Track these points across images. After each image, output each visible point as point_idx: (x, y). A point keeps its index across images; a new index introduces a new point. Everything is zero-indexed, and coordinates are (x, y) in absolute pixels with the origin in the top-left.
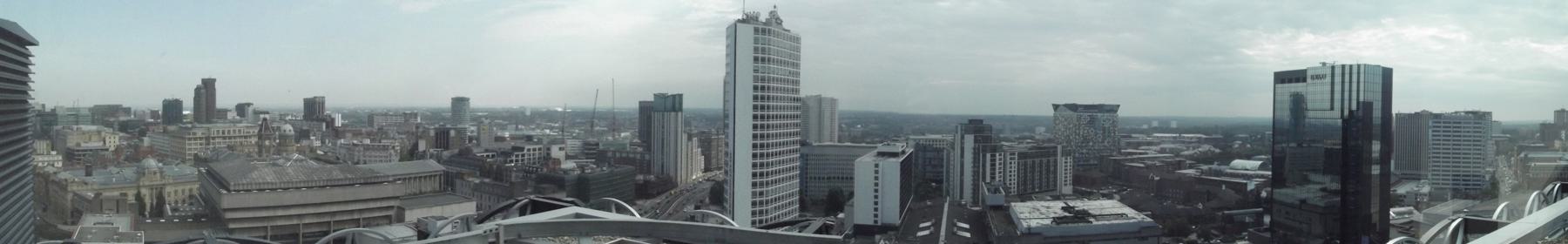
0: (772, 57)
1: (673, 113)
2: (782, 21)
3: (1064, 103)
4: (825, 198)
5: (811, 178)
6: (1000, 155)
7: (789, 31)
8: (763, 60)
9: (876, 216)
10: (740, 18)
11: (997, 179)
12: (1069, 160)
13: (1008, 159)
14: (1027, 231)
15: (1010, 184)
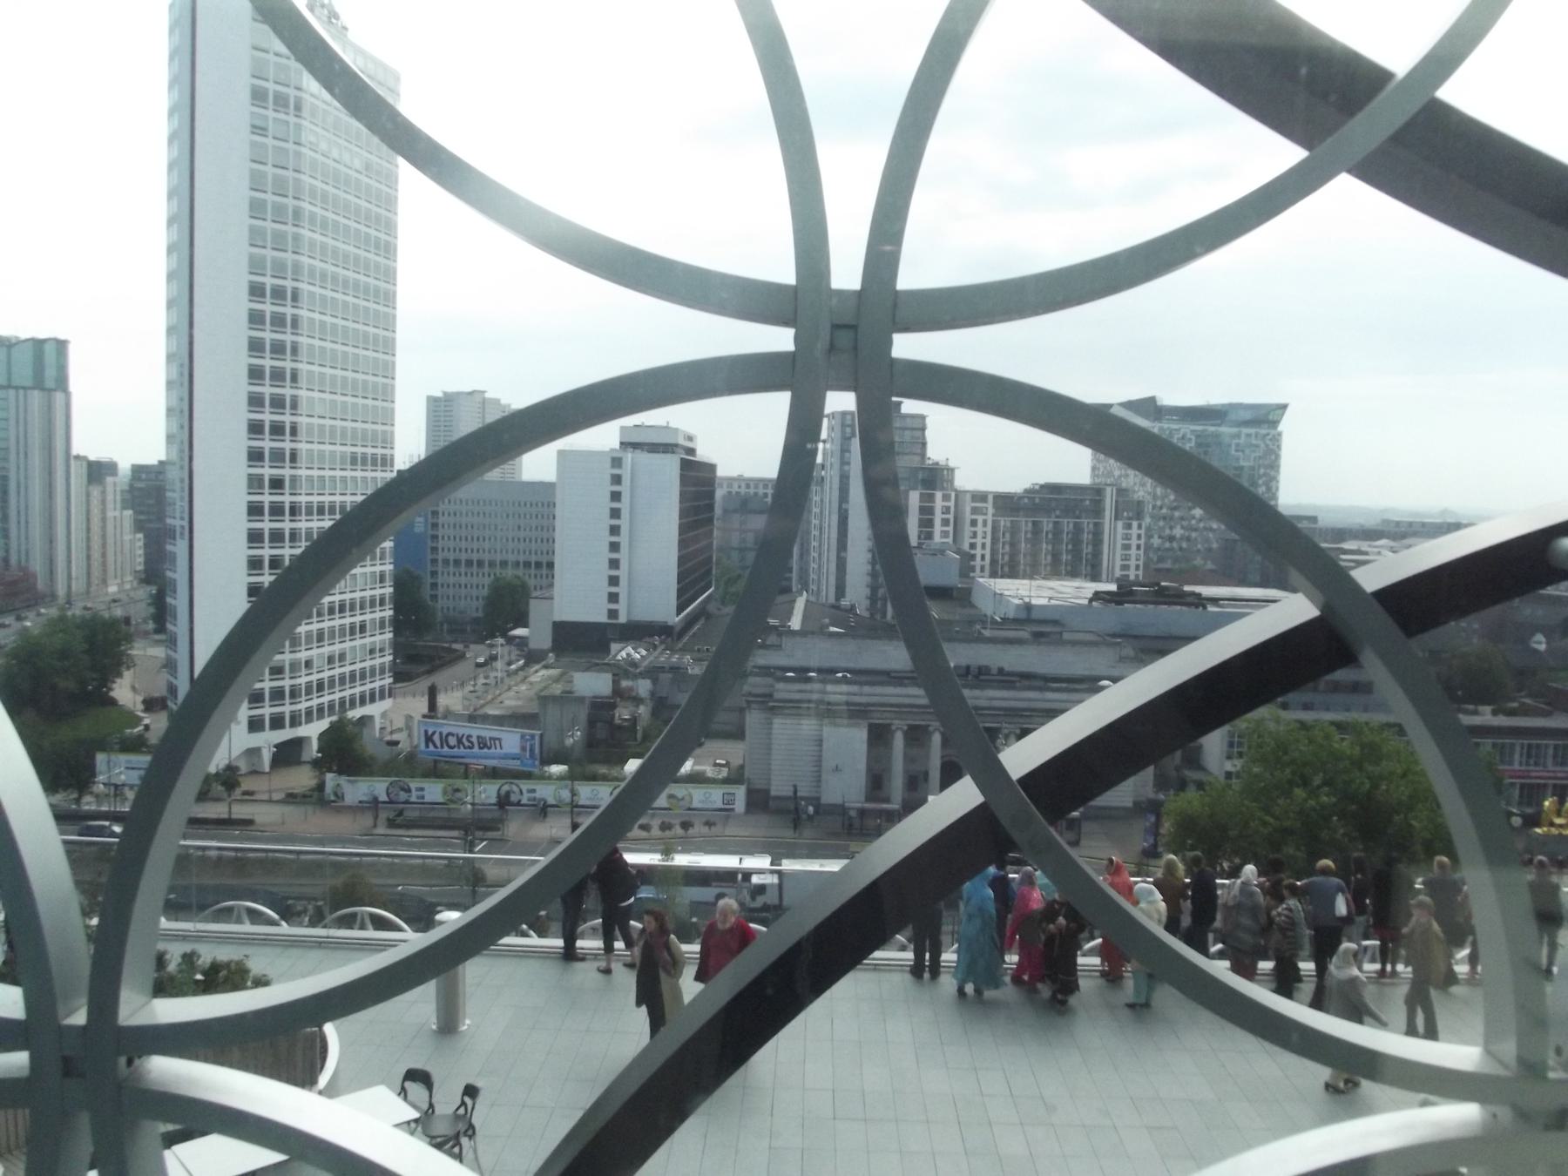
1: (36, 397)
4: (480, 614)
5: (446, 562)
6: (946, 498)
9: (613, 598)
11: (937, 538)
12: (1134, 531)
13: (968, 509)
14: (1023, 615)
15: (973, 546)
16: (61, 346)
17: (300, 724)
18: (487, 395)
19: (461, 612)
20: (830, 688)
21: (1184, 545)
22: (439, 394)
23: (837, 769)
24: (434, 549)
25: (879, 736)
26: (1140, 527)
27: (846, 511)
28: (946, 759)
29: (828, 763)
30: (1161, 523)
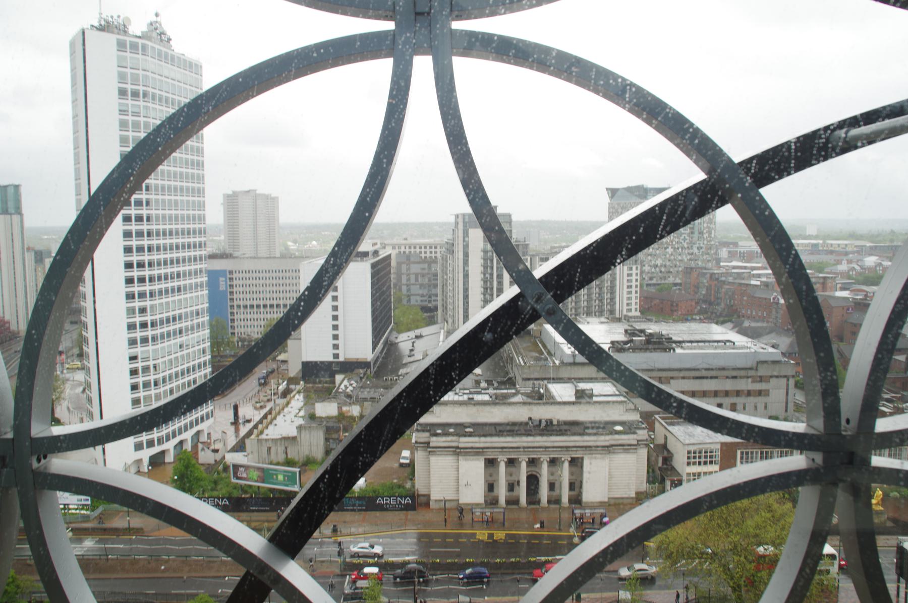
0: (150, 90)
2: (169, 40)
3: (625, 186)
5: (239, 306)
7: (183, 55)
8: (135, 94)
9: (336, 347)
10: (96, 24)
12: (634, 271)
16: (17, 187)
17: (163, 443)
18: (257, 192)
19: (248, 335)
20: (463, 439)
21: (663, 270)
22: (230, 193)
23: (468, 484)
24: (232, 300)
25: (491, 463)
26: (637, 268)
27: (467, 271)
28: (529, 473)
29: (462, 482)
30: (649, 258)
